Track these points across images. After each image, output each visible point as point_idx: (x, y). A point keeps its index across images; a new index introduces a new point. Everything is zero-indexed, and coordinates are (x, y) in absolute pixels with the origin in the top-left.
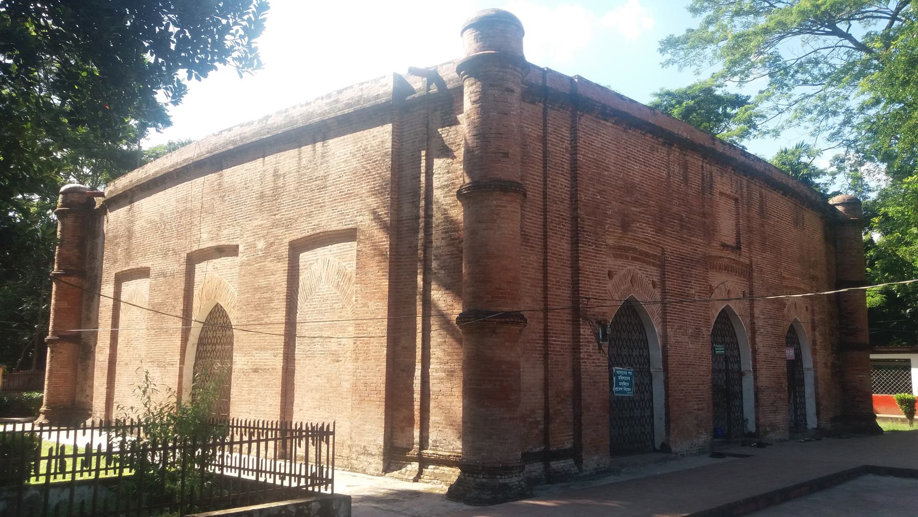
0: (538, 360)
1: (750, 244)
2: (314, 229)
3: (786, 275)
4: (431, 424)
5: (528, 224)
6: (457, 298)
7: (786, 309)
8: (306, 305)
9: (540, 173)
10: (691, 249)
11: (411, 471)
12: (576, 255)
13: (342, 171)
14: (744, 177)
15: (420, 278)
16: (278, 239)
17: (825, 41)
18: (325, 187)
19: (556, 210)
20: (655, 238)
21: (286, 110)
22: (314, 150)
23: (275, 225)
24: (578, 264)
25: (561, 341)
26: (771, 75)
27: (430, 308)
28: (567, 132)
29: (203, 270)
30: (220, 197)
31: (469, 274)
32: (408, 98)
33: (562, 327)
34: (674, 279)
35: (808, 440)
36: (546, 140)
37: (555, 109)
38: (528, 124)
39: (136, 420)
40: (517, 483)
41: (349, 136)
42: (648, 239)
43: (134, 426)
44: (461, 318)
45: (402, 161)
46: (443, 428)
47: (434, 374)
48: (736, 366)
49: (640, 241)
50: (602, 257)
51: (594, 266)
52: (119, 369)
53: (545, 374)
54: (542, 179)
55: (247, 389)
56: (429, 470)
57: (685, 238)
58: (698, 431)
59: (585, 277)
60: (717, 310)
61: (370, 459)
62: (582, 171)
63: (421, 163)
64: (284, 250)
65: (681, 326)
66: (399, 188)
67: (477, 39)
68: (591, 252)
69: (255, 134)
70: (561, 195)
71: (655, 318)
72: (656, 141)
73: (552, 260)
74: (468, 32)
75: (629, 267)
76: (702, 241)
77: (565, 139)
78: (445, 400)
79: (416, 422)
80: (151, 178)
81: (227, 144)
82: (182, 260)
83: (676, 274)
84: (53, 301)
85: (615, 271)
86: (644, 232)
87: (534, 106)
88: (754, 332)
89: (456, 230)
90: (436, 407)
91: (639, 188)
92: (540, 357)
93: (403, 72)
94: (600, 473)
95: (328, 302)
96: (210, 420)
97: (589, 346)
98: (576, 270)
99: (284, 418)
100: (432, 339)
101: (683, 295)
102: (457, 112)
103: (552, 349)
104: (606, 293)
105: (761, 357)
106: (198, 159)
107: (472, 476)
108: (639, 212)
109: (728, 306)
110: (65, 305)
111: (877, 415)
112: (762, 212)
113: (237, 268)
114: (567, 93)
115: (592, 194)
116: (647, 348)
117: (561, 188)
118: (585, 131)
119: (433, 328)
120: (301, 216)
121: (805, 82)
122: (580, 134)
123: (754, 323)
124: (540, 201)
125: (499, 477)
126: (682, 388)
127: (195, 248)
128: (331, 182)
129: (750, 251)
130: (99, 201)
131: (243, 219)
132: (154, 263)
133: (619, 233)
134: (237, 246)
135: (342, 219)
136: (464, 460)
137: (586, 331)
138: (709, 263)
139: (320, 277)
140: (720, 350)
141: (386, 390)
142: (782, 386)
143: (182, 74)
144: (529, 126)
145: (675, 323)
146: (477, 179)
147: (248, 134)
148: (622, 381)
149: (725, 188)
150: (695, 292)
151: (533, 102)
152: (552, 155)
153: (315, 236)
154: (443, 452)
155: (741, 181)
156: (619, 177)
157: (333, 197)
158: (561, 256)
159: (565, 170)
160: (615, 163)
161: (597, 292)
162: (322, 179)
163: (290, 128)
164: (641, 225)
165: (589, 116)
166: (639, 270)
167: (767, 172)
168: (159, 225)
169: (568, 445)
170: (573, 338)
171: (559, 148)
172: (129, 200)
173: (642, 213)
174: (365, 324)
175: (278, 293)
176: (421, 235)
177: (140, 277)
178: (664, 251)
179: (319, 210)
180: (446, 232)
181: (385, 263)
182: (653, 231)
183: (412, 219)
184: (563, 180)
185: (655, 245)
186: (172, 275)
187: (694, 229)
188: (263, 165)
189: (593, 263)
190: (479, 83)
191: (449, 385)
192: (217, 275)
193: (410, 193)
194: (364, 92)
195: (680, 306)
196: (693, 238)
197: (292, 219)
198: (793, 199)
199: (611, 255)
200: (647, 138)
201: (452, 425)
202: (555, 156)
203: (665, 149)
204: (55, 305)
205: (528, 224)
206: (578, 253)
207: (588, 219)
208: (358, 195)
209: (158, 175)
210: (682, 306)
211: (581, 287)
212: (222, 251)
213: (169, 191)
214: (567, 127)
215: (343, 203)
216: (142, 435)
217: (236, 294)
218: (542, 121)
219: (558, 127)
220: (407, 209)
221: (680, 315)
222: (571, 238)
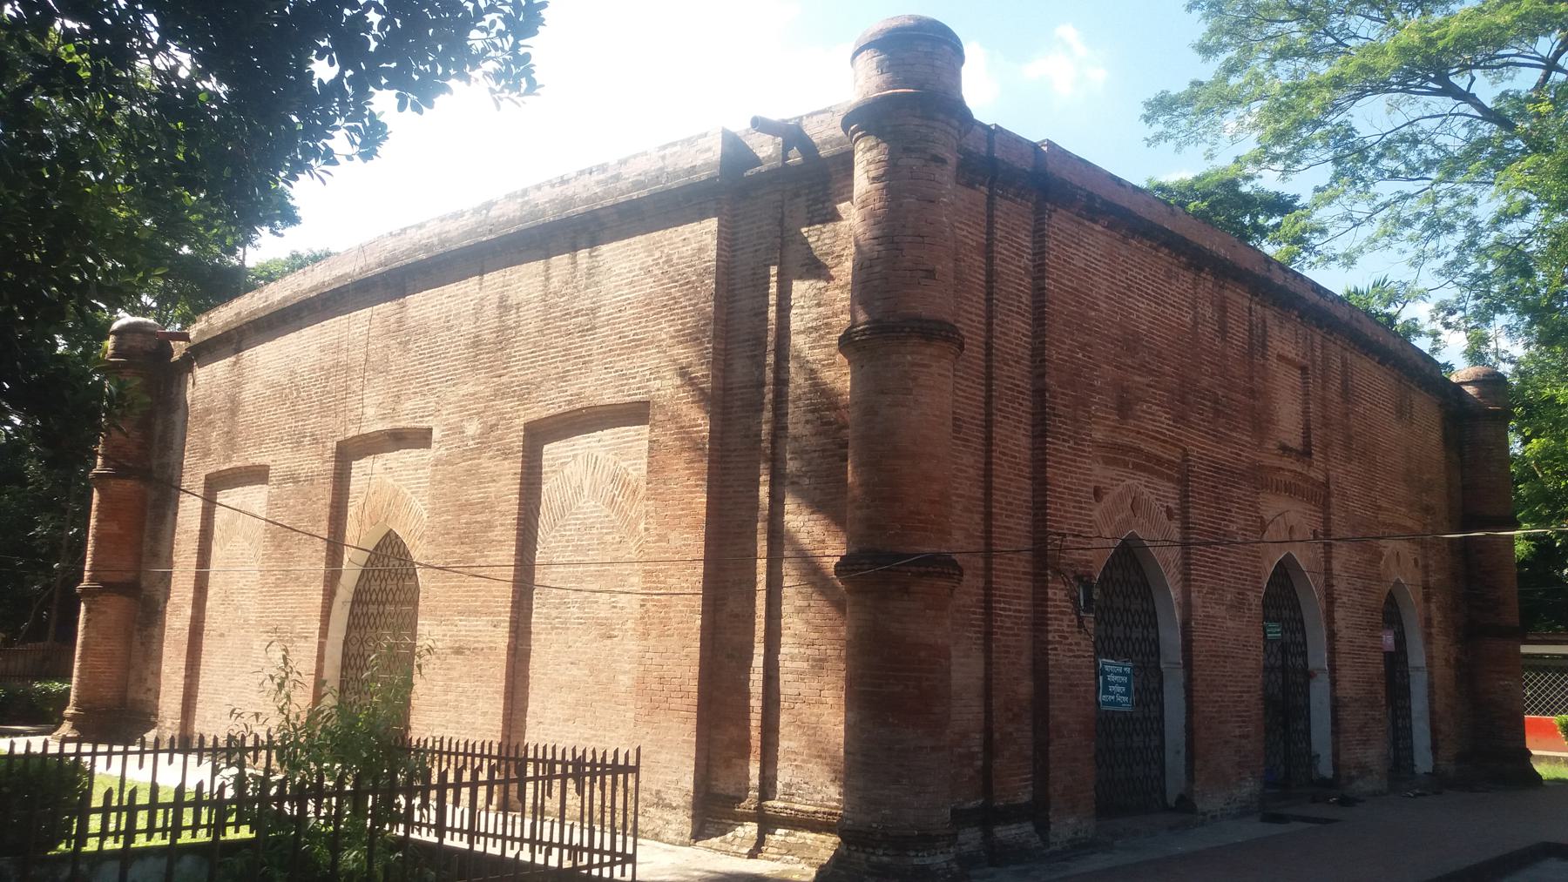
0: (975, 644)
1: (1326, 447)
2: (570, 402)
3: (1383, 503)
4: (780, 754)
5: (960, 399)
6: (832, 528)
7: (1382, 562)
8: (554, 537)
9: (980, 309)
10: (1231, 452)
11: (743, 838)
12: (1041, 457)
13: (625, 300)
14: (1318, 330)
15: (764, 491)
16: (505, 419)
17: (1427, 105)
18: (594, 328)
19: (1009, 377)
20: (1172, 432)
21: (525, 192)
22: (574, 263)
23: (500, 393)
24: (1045, 472)
25: (1015, 611)
26: (1336, 161)
27: (782, 545)
28: (1027, 239)
29: (364, 471)
30: (400, 343)
31: (861, 485)
32: (749, 173)
33: (1015, 585)
34: (1204, 505)
35: (1419, 795)
36: (992, 252)
37: (1006, 198)
38: (961, 223)
39: (263, 737)
40: (944, 865)
41: (638, 238)
42: (1161, 433)
43: (261, 749)
44: (844, 566)
45: (734, 284)
46: (803, 761)
47: (788, 664)
48: (1300, 661)
49: (1148, 436)
50: (1085, 463)
51: (1072, 478)
52: (208, 644)
53: (986, 669)
54: (983, 321)
55: (441, 683)
56: (777, 837)
57: (1221, 433)
58: (1240, 773)
59: (1057, 497)
60: (1271, 563)
61: (668, 815)
62: (1053, 309)
63: (768, 288)
64: (516, 439)
65: (1214, 589)
66: (728, 332)
67: (881, 68)
68: (1066, 453)
69: (467, 234)
70: (1016, 351)
71: (1170, 574)
72: (1176, 262)
73: (1001, 466)
74: (865, 55)
75: (1129, 482)
76: (1248, 439)
77: (1024, 252)
78: (808, 711)
79: (753, 749)
80: (275, 308)
81: (416, 250)
82: (328, 454)
83: (1207, 496)
84: (93, 522)
85: (1105, 488)
86: (1154, 421)
87: (973, 191)
88: (1330, 600)
89: (834, 406)
90: (789, 724)
91: (1147, 341)
92: (978, 638)
93: (740, 125)
94: (1079, 848)
95: (594, 531)
96: (396, 741)
97: (1062, 620)
98: (1040, 483)
99: (509, 737)
100: (784, 601)
101: (1217, 533)
102: (837, 199)
103: (999, 624)
104: (1091, 527)
105: (1342, 646)
106: (361, 277)
107: (864, 852)
108: (1147, 385)
109: (1289, 556)
110: (114, 528)
111: (1533, 752)
112: (1347, 392)
113: (429, 470)
114: (1028, 170)
115: (1069, 350)
116: (1155, 626)
117: (1016, 338)
118: (1059, 238)
119: (787, 582)
120: (547, 378)
121: (1394, 175)
122: (1050, 243)
123: (1333, 586)
124: (979, 359)
125: (912, 854)
126: (1215, 699)
127: (353, 432)
128: (603, 319)
129: (1327, 459)
130: (179, 349)
131: (442, 382)
132: (278, 459)
133: (1113, 421)
134: (430, 430)
135: (622, 385)
136: (848, 822)
137: (1057, 593)
138: (1260, 478)
139: (581, 487)
140: (1275, 631)
141: (700, 691)
142: (1376, 698)
143: (383, 101)
144: (964, 227)
145: (1204, 582)
146: (877, 317)
147: (454, 234)
148: (1113, 684)
149: (1286, 347)
150: (1237, 528)
151: (970, 185)
152: (1002, 278)
153: (572, 415)
154: (802, 805)
155: (1311, 335)
156: (1112, 322)
157: (607, 346)
158: (1015, 457)
159: (1023, 307)
160: (1107, 297)
161: (1076, 525)
162: (587, 314)
163: (530, 224)
164: (1150, 408)
165: (1064, 212)
166: (1146, 486)
167: (1355, 324)
168: (287, 390)
169: (1024, 797)
170: (1035, 605)
171: (1014, 267)
172: (234, 346)
173: (1151, 386)
174: (661, 571)
175: (503, 514)
176: (767, 415)
177: (250, 483)
178: (1188, 455)
179: (580, 369)
180: (813, 411)
181: (701, 464)
182: (1169, 419)
183: (752, 386)
184: (1019, 323)
185: (1172, 444)
186: (310, 480)
187: (1236, 417)
188: (480, 289)
189: (1070, 472)
190: (884, 145)
191: (815, 684)
192: (390, 481)
193: (749, 340)
194: (666, 162)
195: (1213, 553)
196: (1235, 434)
197: (532, 384)
198: (1396, 371)
199: (1099, 459)
200: (1160, 255)
201: (820, 757)
202: (1008, 280)
203: (1189, 276)
204: (97, 528)
205: (960, 399)
206: (1046, 454)
207: (1063, 394)
208: (652, 342)
209: (289, 304)
210: (1215, 553)
211: (1051, 515)
212: (399, 439)
213: (308, 332)
214: (1028, 231)
215: (625, 357)
216: (275, 765)
217: (425, 515)
218: (985, 218)
219: (1013, 229)
220: (741, 368)
221: (1213, 568)
222: (1033, 426)
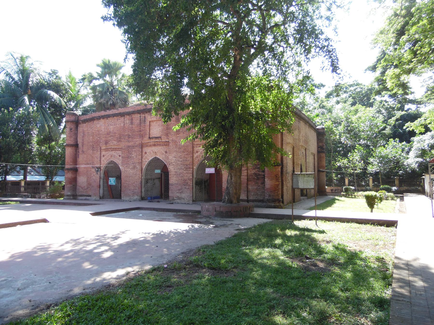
203: (123, 118)
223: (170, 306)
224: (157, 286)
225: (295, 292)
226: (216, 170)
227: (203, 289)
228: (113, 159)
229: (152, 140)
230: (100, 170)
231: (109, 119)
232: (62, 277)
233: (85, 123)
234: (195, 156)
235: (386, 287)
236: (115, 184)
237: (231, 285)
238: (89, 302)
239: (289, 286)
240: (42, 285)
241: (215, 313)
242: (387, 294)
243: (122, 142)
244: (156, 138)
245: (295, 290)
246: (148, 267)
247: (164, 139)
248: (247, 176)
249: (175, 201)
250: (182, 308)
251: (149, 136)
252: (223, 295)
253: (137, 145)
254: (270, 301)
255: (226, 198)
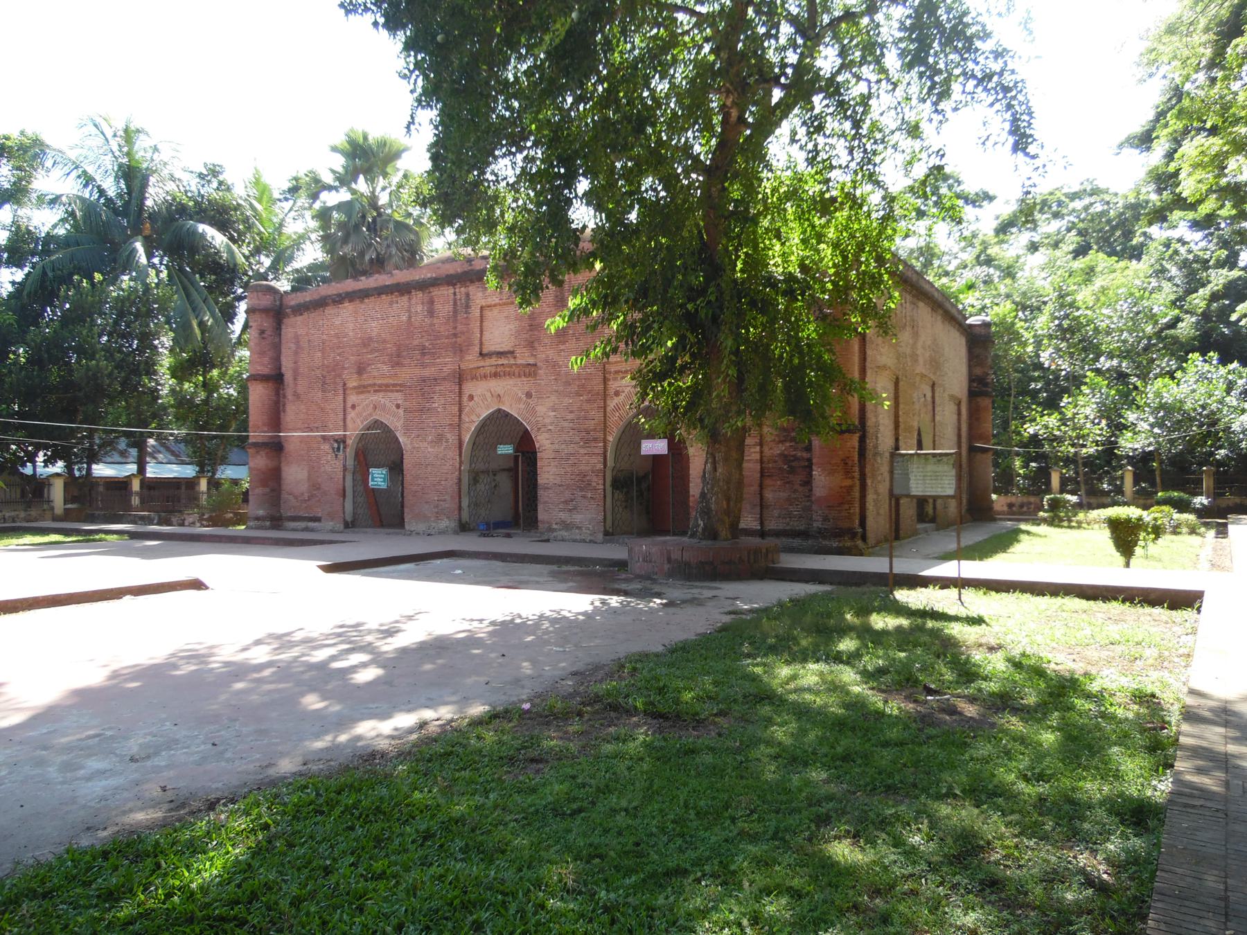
203: (405, 298)
223: (537, 811)
224: (501, 758)
225: (890, 781)
226: (671, 445)
227: (629, 769)
228: (378, 416)
229: (488, 362)
230: (345, 448)
231: (366, 301)
232: (245, 730)
233: (301, 314)
234: (612, 404)
235: (1157, 771)
236: (385, 487)
237: (708, 759)
238: (318, 795)
239: (875, 764)
240: (194, 749)
241: (663, 830)
242: (1161, 788)
243: (403, 365)
244: (500, 354)
245: (890, 775)
246: (478, 710)
247: (524, 358)
248: (761, 461)
249: (555, 534)
250: (571, 815)
251: (481, 349)
252: (685, 784)
253: (445, 374)
254: (819, 803)
255: (699, 525)
